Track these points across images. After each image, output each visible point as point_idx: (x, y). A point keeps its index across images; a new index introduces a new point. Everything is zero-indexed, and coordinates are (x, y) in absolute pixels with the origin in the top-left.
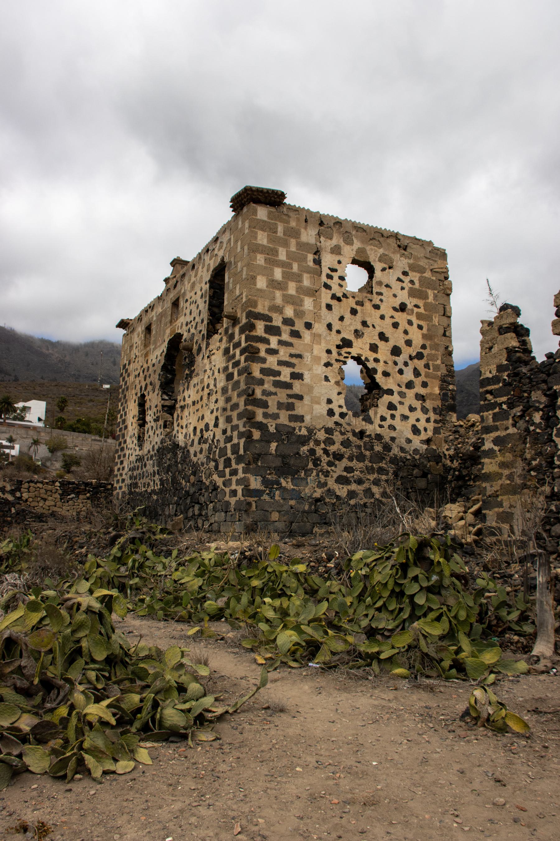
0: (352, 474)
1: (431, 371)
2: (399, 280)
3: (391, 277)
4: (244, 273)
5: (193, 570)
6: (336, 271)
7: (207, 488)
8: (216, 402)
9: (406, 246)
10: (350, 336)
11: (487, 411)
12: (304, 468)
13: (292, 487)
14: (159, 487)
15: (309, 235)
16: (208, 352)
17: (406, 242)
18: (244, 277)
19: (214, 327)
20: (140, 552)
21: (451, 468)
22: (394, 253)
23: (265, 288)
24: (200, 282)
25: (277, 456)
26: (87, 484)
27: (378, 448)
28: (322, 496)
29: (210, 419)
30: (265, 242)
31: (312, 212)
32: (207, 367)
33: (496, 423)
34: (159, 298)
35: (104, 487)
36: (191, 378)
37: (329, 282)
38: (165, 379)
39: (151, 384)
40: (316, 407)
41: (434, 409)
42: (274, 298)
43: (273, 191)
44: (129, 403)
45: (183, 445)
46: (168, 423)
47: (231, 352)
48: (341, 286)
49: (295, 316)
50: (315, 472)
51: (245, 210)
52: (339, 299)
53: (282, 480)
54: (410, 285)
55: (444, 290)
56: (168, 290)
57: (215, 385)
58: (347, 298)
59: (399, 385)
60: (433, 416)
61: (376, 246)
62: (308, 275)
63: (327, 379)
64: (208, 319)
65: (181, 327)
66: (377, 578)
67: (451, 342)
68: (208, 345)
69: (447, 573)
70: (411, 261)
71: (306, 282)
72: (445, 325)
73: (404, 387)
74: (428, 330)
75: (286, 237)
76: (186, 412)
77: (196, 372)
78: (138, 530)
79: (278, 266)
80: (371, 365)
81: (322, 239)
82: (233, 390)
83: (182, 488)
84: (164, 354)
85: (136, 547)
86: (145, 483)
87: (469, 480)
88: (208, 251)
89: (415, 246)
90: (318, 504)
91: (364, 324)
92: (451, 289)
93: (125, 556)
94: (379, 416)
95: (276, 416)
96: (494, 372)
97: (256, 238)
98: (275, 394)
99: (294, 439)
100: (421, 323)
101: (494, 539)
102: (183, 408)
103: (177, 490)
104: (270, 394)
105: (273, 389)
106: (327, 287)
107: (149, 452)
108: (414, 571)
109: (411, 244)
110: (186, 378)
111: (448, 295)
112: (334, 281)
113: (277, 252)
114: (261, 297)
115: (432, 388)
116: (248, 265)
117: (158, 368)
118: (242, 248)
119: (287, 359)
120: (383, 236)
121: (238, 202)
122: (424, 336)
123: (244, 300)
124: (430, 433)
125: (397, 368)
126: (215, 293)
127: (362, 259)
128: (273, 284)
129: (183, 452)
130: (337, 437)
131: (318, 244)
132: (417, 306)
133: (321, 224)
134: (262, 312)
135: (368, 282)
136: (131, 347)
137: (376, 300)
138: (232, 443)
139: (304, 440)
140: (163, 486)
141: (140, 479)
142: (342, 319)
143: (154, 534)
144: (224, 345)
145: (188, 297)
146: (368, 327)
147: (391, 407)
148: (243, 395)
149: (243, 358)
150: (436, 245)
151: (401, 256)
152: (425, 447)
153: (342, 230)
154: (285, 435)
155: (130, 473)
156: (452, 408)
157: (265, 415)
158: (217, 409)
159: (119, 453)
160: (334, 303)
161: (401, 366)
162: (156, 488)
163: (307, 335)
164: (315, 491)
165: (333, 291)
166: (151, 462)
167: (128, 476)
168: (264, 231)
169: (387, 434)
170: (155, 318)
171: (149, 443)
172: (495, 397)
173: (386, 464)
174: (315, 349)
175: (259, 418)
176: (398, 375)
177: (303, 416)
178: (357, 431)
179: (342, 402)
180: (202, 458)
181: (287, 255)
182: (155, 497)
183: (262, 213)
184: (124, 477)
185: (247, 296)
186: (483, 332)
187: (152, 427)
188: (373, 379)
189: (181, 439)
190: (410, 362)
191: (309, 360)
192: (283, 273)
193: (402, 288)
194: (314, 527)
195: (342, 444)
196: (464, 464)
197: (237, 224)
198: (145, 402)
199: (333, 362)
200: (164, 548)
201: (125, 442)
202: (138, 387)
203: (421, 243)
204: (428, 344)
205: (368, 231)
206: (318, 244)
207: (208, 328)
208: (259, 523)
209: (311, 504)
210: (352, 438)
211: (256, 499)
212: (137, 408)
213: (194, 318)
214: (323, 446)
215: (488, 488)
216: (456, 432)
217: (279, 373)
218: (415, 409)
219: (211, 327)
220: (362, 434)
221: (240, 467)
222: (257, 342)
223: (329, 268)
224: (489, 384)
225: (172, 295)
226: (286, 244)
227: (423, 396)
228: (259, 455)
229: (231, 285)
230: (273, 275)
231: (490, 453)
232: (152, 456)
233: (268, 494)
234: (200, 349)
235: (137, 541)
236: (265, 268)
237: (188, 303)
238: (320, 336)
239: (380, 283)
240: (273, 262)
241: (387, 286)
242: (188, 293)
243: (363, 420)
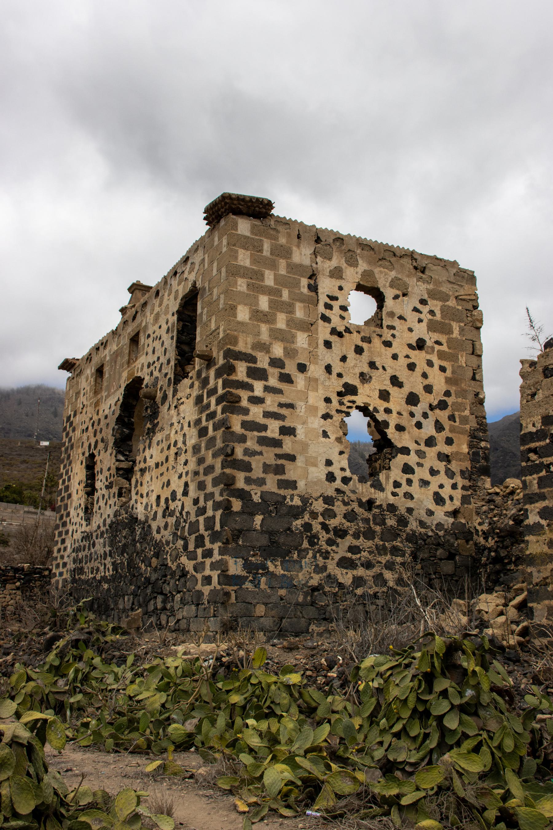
0: (358, 556)
1: (457, 424)
2: (416, 310)
3: (405, 306)
4: (222, 301)
5: (154, 682)
6: (336, 299)
7: (173, 574)
8: (186, 463)
9: (425, 268)
10: (355, 381)
11: (531, 475)
12: (297, 547)
13: (282, 572)
14: (111, 572)
15: (302, 255)
16: (176, 401)
17: (424, 263)
18: (221, 306)
19: (183, 370)
20: (85, 658)
21: (485, 548)
22: (408, 276)
23: (248, 321)
24: (166, 313)
25: (262, 532)
26: (17, 570)
27: (391, 522)
28: (320, 584)
29: (177, 485)
30: (247, 263)
31: (306, 226)
32: (175, 420)
33: (542, 490)
34: (114, 333)
35: (39, 573)
36: (154, 433)
37: (328, 313)
38: (120, 434)
39: (103, 440)
40: (312, 469)
41: (462, 473)
42: (259, 334)
43: (258, 199)
44: (73, 465)
46: (124, 490)
47: (205, 401)
48: (343, 318)
49: (285, 355)
50: (311, 552)
51: (222, 222)
52: (340, 335)
53: (269, 563)
54: (430, 317)
55: (473, 322)
56: (125, 323)
57: (184, 443)
58: (350, 333)
59: (416, 442)
60: (460, 481)
61: (386, 267)
62: (302, 305)
63: (325, 434)
64: (176, 359)
65: (142, 369)
66: (394, 692)
67: (482, 387)
68: (175, 391)
69: (485, 686)
70: (431, 287)
71: (299, 313)
72: (475, 366)
73: (423, 444)
74: (453, 372)
75: (274, 257)
76: (147, 477)
77: (160, 425)
78: (82, 629)
79: (264, 293)
80: (381, 417)
81: (319, 259)
82: (207, 448)
83: (141, 574)
84: (120, 403)
85: (79, 652)
86: (92, 568)
87: (510, 563)
88: (175, 274)
89: (435, 268)
90: (316, 593)
91: (372, 365)
92: (481, 321)
93: (64, 664)
94: (391, 481)
95: (261, 482)
96: (539, 425)
97: (236, 258)
98: (261, 453)
99: (284, 510)
100: (444, 364)
101: (545, 641)
102: (143, 471)
103: (134, 576)
104: (254, 453)
105: (258, 448)
106: (325, 319)
107: (99, 527)
108: (442, 684)
109: (430, 265)
110: (148, 434)
111: (478, 328)
112: (334, 312)
113: (263, 275)
114: (243, 332)
115: (459, 445)
116: (226, 292)
117: (112, 421)
118: (219, 271)
119: (275, 409)
120: (395, 255)
121: (213, 213)
122: (448, 381)
123: (221, 335)
124: (457, 503)
125: (414, 421)
126: (184, 326)
127: (369, 285)
128: (258, 316)
129: (143, 528)
130: (339, 508)
131: (314, 265)
132: (438, 343)
133: (318, 240)
134: (243, 350)
135: (377, 313)
136: (78, 393)
137: (387, 335)
138: (206, 516)
139: (297, 513)
140: (117, 572)
141: (86, 563)
142: (344, 359)
143: (104, 634)
144: (195, 392)
145: (150, 331)
146: (378, 369)
147: (407, 469)
148: (219, 456)
149: (219, 408)
150: (462, 266)
151: (418, 281)
152: (451, 520)
153: (343, 248)
154: (273, 505)
155: (74, 554)
156: (485, 471)
157: (248, 480)
158: (187, 473)
159: (60, 529)
160: (334, 339)
161: (418, 417)
162: (107, 574)
163: (300, 380)
164: (312, 578)
165: (332, 325)
166: (102, 540)
167: (72, 558)
168: (247, 249)
169: (402, 504)
170: (108, 358)
171: (99, 515)
172: (540, 457)
173: (401, 542)
174: (310, 396)
175: (240, 484)
176: (415, 429)
177: (296, 482)
178: (364, 500)
179: (345, 463)
180: (167, 535)
181: (275, 279)
182: (106, 586)
183: (244, 226)
184: (66, 559)
185: (224, 331)
186: (523, 375)
187: (104, 496)
188: (384, 435)
189: (140, 511)
190: (430, 413)
191: (303, 410)
192: (270, 301)
193: (420, 321)
194: (310, 624)
195: (345, 516)
196: (502, 542)
197: (213, 240)
198: (95, 463)
199: (333, 413)
200: (117, 653)
201: (68, 515)
202: (86, 445)
203: (442, 264)
204: (453, 389)
205: (376, 249)
206: (314, 265)
207: (175, 370)
208: (239, 620)
209: (306, 595)
210: (358, 510)
211: (235, 588)
212: (84, 471)
213: (159, 358)
214: (321, 519)
215: (535, 574)
216: (490, 501)
217: (264, 428)
218: (438, 472)
219: (179, 369)
220: (370, 504)
221: (216, 547)
222: (237, 388)
223: (328, 296)
224: (532, 441)
225: (130, 329)
226: (273, 266)
227: (447, 456)
228: (240, 531)
229: (204, 317)
230: (257, 304)
231: (536, 529)
232: (102, 533)
233: (251, 581)
234: (165, 397)
235: (81, 644)
236: (247, 295)
237: (151, 339)
238: (316, 380)
239: (391, 314)
240: (256, 287)
241: (401, 318)
242: (150, 326)
243: (372, 486)
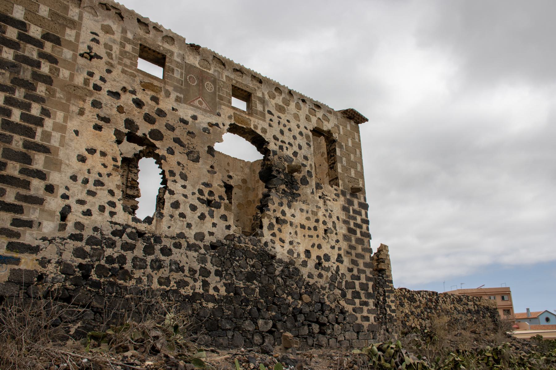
45: (287, 260)
162: (211, 292)
232: (190, 247)
